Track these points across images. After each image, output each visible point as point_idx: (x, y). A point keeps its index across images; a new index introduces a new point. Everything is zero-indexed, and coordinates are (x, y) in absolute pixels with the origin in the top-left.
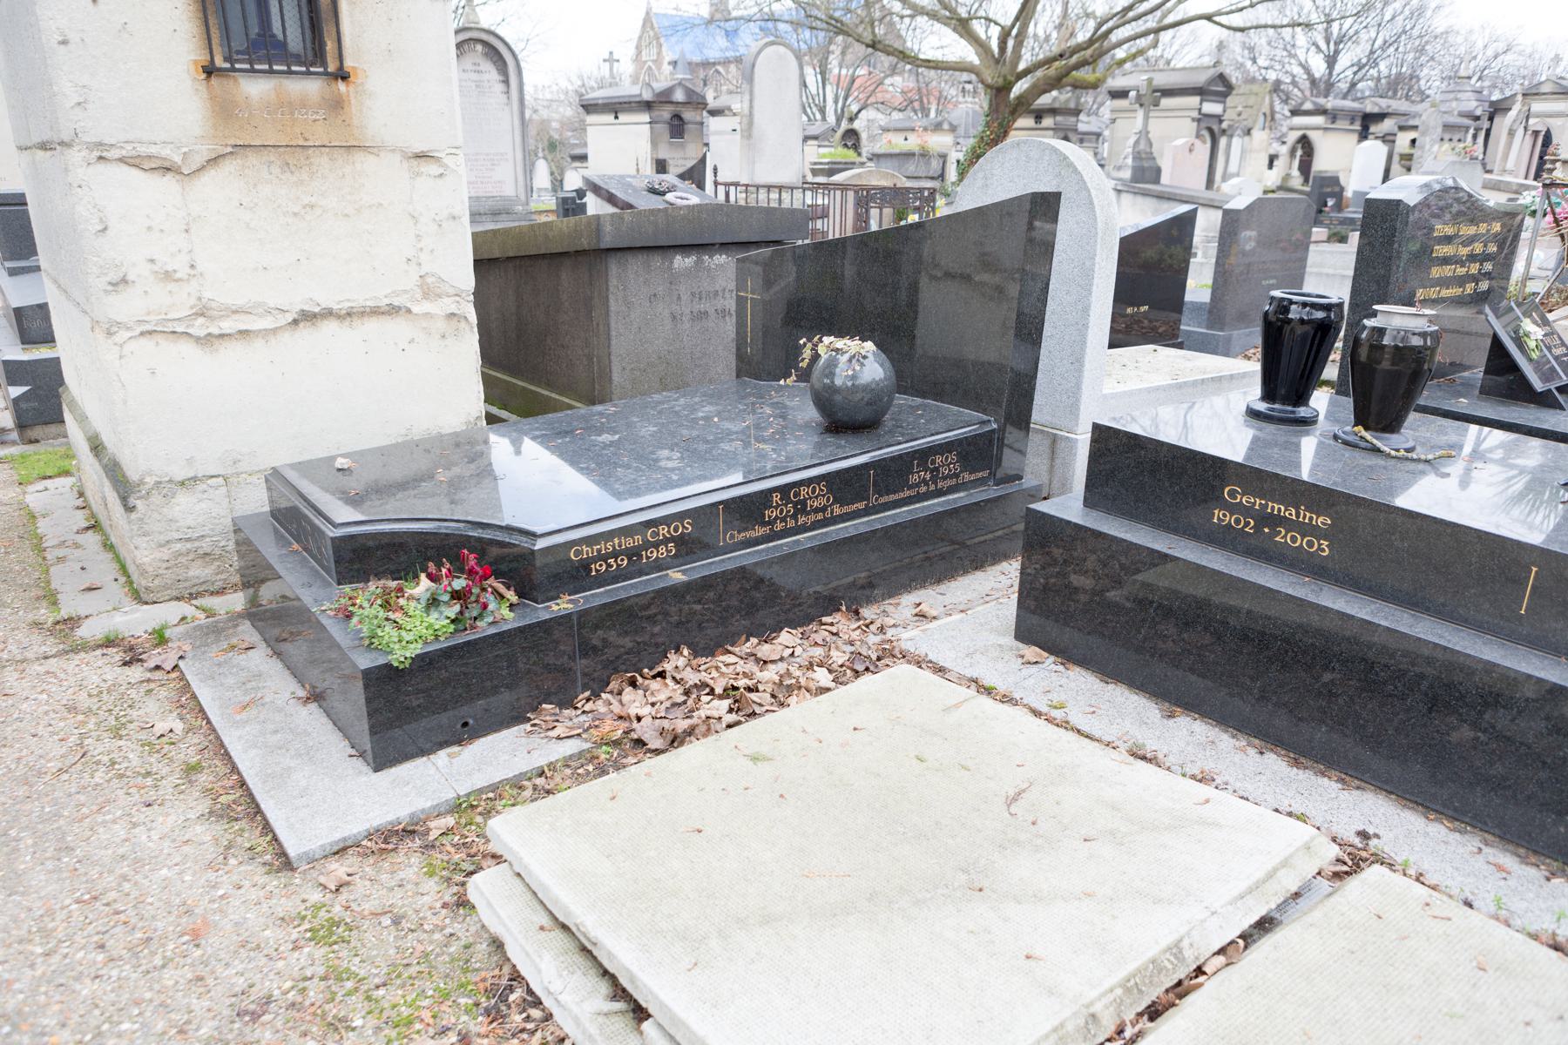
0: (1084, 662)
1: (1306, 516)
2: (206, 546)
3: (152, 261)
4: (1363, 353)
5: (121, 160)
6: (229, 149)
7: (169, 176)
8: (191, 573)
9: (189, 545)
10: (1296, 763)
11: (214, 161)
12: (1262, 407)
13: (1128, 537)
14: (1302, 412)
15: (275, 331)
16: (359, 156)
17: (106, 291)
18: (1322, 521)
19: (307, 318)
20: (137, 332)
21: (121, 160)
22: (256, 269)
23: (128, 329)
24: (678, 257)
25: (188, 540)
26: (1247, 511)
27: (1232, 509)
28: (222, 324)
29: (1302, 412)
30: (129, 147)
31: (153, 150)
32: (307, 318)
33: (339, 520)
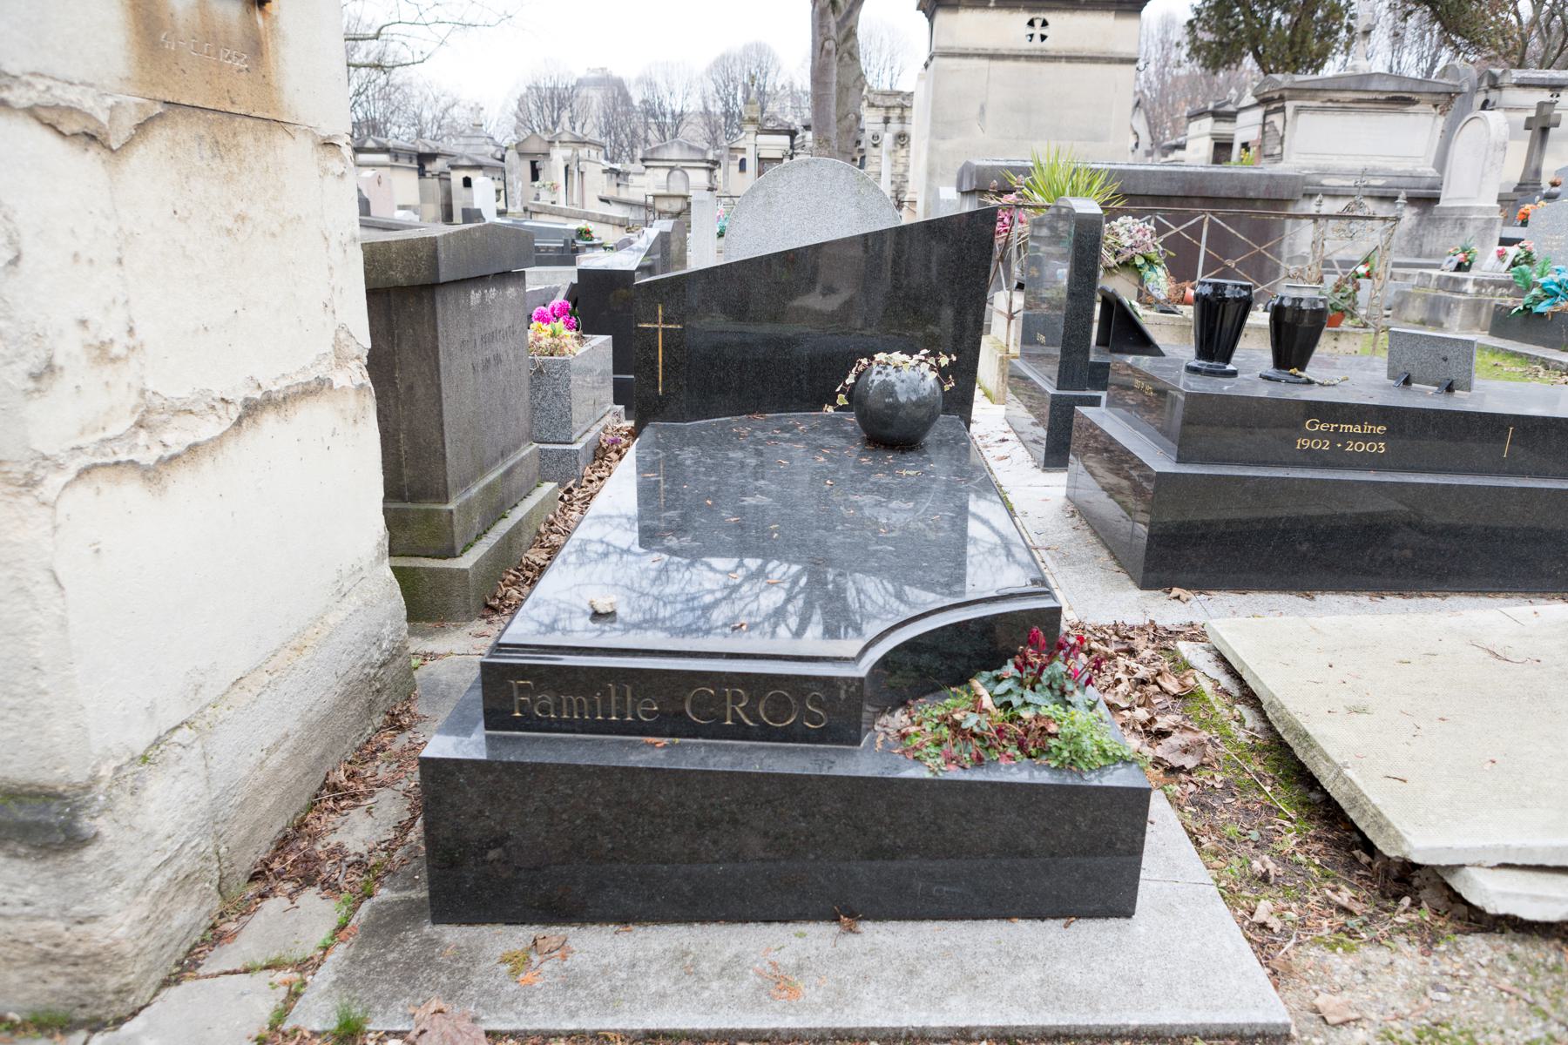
0: (1218, 587)
1: (1368, 428)
2: (186, 863)
3: (83, 323)
4: (1288, 317)
5: (32, 112)
6: (159, 109)
7: (94, 149)
8: (176, 924)
9: (169, 872)
10: (1404, 597)
11: (142, 127)
12: (1195, 363)
13: (1266, 474)
14: (1230, 367)
15: (219, 440)
16: (279, 137)
17: (27, 392)
18: (1380, 429)
19: (252, 409)
20: (71, 474)
21: (32, 112)
22: (196, 331)
23: (59, 467)
24: (493, 290)
25: (166, 863)
26: (1323, 435)
27: (1311, 436)
28: (168, 438)
29: (1230, 367)
30: (41, 85)
31: (71, 96)
32: (252, 409)
33: (854, 654)
